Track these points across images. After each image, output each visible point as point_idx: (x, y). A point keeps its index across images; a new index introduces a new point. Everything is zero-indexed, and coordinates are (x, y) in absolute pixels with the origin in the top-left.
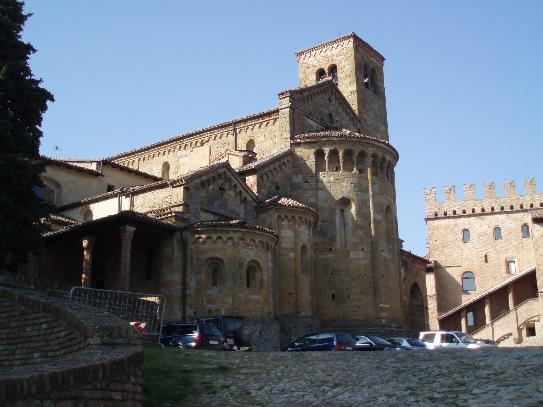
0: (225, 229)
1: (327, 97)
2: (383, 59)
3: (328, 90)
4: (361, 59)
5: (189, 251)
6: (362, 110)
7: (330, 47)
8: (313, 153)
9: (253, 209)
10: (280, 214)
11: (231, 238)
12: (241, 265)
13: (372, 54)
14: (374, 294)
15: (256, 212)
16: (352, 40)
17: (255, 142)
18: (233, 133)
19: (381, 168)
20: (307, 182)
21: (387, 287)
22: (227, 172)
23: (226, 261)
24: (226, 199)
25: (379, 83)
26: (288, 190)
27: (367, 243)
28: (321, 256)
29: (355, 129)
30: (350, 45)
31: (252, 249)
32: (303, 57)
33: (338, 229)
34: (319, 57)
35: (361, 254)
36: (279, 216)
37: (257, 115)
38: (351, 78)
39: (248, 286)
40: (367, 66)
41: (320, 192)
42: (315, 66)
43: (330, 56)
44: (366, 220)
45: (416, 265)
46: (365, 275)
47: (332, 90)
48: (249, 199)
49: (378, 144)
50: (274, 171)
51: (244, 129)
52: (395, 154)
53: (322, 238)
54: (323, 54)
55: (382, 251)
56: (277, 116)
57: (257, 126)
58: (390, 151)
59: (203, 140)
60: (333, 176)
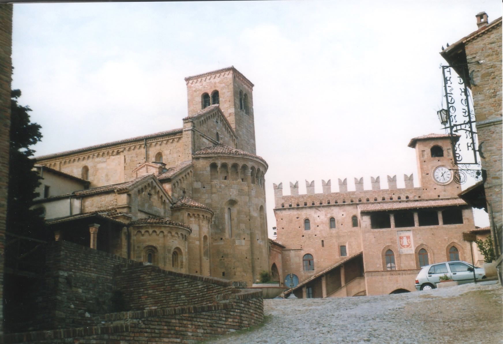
0: (158, 225)
1: (215, 120)
2: (252, 85)
3: (216, 114)
4: (237, 87)
5: (132, 241)
6: (238, 128)
7: (213, 76)
8: (209, 165)
9: (170, 209)
10: (189, 213)
11: (162, 232)
12: (169, 251)
13: (245, 82)
14: (252, 272)
15: (171, 211)
16: (231, 72)
17: (163, 155)
18: (144, 146)
19: (257, 177)
20: (204, 188)
21: (261, 267)
22: (154, 181)
23: (159, 248)
24: (152, 202)
25: (250, 105)
26: (191, 194)
27: (248, 234)
28: (215, 244)
29: (233, 143)
30: (230, 76)
31: (176, 240)
32: (191, 82)
33: (227, 223)
34: (204, 83)
35: (243, 242)
36: (189, 214)
37: (165, 134)
38: (230, 103)
39: (173, 266)
41: (213, 195)
43: (213, 83)
44: (247, 217)
46: (246, 258)
47: (218, 114)
48: (167, 201)
50: (182, 179)
51: (154, 144)
52: (266, 166)
53: (215, 230)
54: (208, 81)
55: (258, 240)
56: (181, 136)
57: (165, 142)
58: (263, 165)
59: (119, 150)
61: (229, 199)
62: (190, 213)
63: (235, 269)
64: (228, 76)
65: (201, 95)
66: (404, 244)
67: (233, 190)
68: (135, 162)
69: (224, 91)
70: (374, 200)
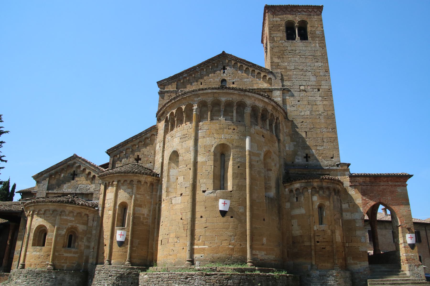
27: (186, 187)
35: (179, 199)
40: (292, 22)
45: (382, 183)
46: (181, 219)
49: (201, 92)
63: (169, 235)
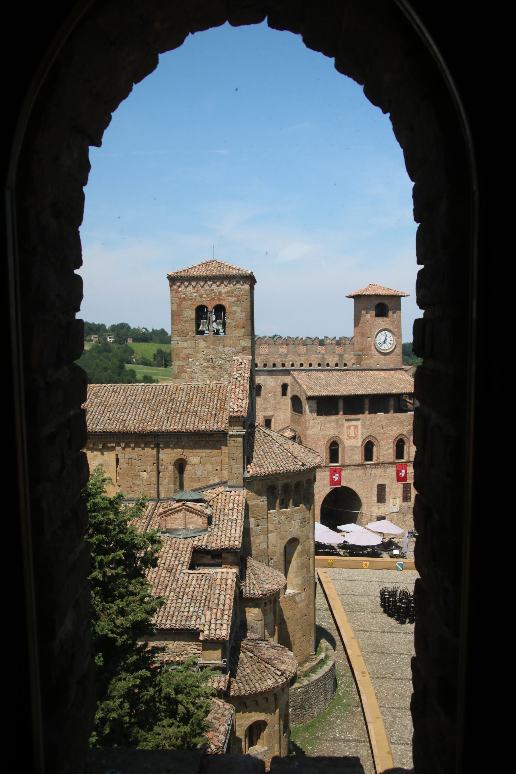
20: (258, 525)
32: (178, 284)
34: (202, 291)
42: (195, 299)
43: (215, 292)
54: (207, 287)
56: (221, 439)
60: (283, 515)
61: (290, 537)
62: (266, 601)
64: (243, 287)
65: (195, 307)
66: (351, 435)
67: (295, 522)
68: (137, 467)
69: (235, 308)
70: (308, 365)
